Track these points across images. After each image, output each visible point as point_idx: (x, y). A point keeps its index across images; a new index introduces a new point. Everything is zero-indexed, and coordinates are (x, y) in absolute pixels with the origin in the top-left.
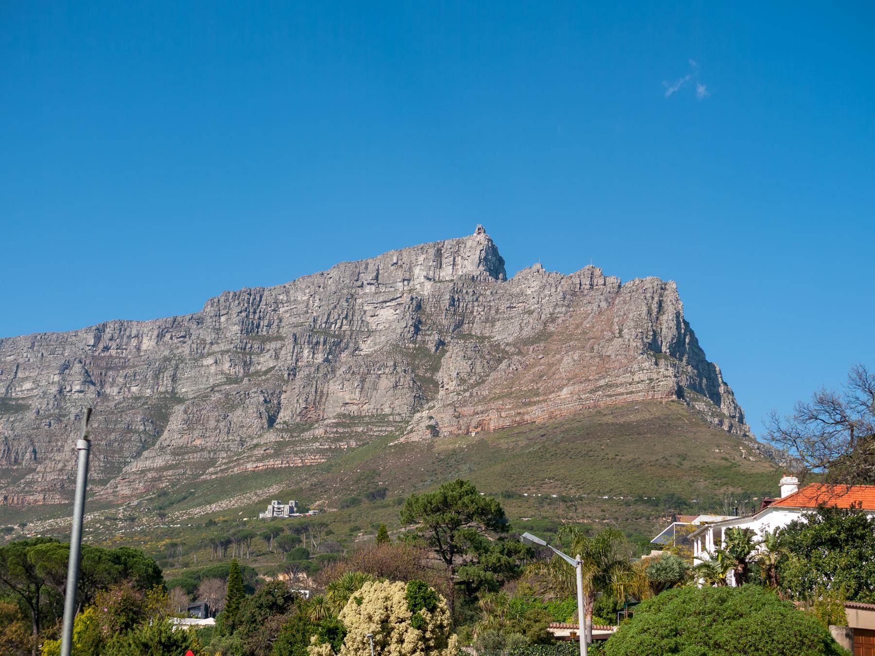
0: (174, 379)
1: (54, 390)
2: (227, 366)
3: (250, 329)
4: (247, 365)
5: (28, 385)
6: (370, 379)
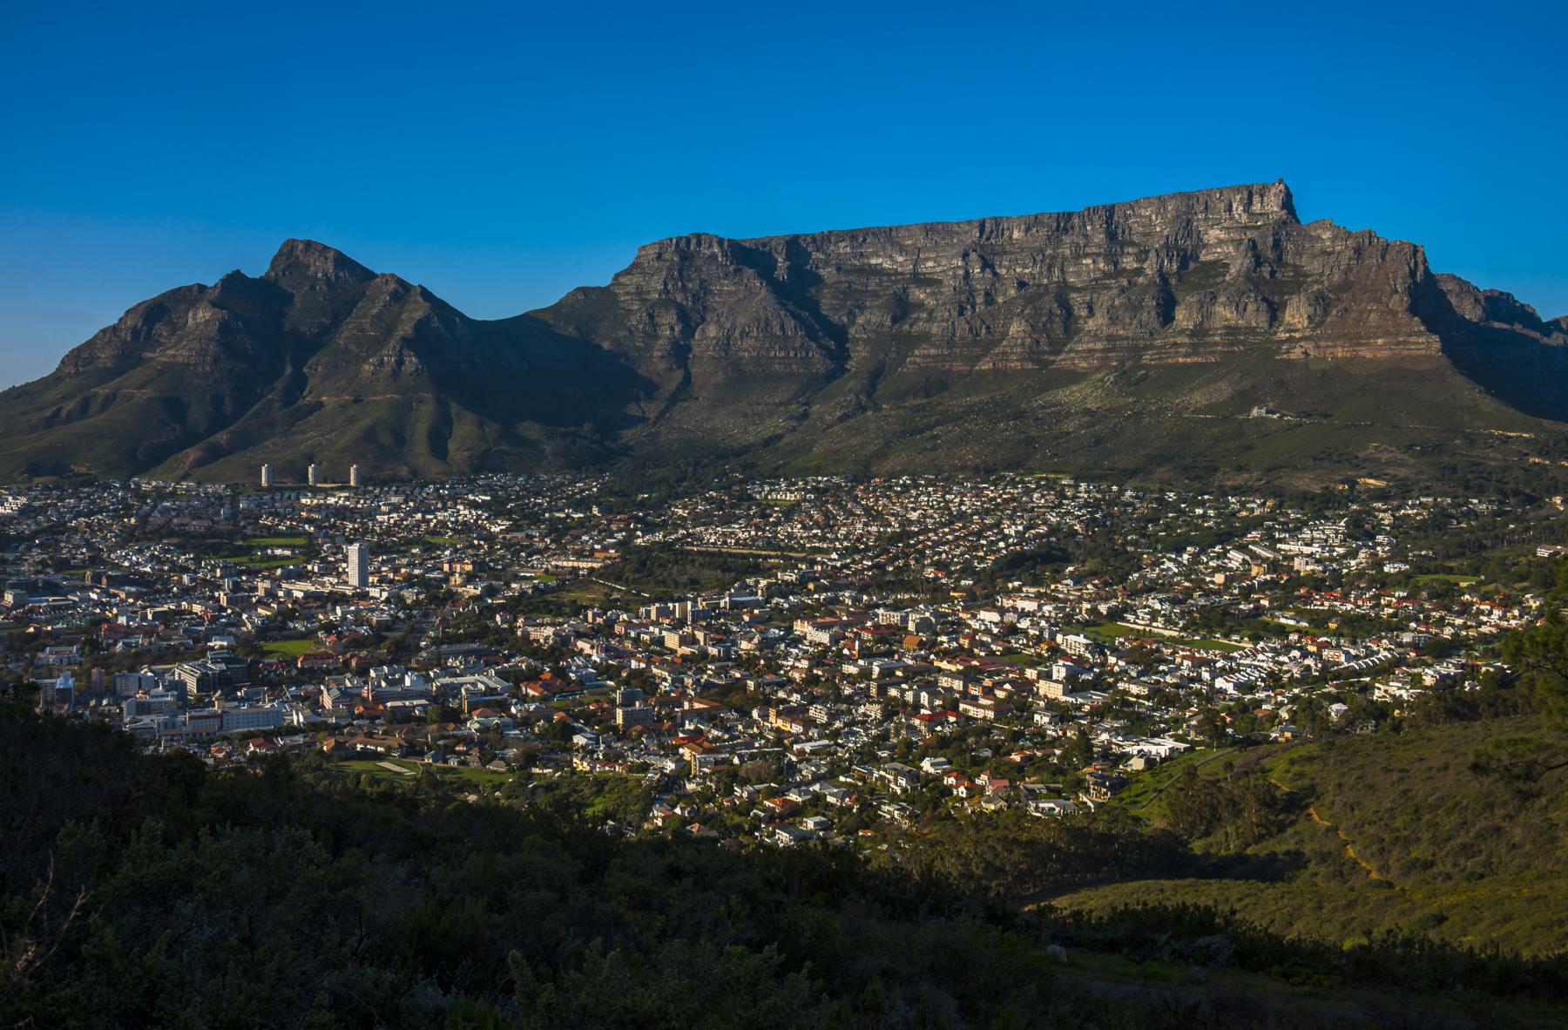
0: (1063, 271)
1: (961, 272)
2: (1101, 265)
3: (1111, 236)
4: (1116, 264)
5: (930, 264)
6: (1241, 306)
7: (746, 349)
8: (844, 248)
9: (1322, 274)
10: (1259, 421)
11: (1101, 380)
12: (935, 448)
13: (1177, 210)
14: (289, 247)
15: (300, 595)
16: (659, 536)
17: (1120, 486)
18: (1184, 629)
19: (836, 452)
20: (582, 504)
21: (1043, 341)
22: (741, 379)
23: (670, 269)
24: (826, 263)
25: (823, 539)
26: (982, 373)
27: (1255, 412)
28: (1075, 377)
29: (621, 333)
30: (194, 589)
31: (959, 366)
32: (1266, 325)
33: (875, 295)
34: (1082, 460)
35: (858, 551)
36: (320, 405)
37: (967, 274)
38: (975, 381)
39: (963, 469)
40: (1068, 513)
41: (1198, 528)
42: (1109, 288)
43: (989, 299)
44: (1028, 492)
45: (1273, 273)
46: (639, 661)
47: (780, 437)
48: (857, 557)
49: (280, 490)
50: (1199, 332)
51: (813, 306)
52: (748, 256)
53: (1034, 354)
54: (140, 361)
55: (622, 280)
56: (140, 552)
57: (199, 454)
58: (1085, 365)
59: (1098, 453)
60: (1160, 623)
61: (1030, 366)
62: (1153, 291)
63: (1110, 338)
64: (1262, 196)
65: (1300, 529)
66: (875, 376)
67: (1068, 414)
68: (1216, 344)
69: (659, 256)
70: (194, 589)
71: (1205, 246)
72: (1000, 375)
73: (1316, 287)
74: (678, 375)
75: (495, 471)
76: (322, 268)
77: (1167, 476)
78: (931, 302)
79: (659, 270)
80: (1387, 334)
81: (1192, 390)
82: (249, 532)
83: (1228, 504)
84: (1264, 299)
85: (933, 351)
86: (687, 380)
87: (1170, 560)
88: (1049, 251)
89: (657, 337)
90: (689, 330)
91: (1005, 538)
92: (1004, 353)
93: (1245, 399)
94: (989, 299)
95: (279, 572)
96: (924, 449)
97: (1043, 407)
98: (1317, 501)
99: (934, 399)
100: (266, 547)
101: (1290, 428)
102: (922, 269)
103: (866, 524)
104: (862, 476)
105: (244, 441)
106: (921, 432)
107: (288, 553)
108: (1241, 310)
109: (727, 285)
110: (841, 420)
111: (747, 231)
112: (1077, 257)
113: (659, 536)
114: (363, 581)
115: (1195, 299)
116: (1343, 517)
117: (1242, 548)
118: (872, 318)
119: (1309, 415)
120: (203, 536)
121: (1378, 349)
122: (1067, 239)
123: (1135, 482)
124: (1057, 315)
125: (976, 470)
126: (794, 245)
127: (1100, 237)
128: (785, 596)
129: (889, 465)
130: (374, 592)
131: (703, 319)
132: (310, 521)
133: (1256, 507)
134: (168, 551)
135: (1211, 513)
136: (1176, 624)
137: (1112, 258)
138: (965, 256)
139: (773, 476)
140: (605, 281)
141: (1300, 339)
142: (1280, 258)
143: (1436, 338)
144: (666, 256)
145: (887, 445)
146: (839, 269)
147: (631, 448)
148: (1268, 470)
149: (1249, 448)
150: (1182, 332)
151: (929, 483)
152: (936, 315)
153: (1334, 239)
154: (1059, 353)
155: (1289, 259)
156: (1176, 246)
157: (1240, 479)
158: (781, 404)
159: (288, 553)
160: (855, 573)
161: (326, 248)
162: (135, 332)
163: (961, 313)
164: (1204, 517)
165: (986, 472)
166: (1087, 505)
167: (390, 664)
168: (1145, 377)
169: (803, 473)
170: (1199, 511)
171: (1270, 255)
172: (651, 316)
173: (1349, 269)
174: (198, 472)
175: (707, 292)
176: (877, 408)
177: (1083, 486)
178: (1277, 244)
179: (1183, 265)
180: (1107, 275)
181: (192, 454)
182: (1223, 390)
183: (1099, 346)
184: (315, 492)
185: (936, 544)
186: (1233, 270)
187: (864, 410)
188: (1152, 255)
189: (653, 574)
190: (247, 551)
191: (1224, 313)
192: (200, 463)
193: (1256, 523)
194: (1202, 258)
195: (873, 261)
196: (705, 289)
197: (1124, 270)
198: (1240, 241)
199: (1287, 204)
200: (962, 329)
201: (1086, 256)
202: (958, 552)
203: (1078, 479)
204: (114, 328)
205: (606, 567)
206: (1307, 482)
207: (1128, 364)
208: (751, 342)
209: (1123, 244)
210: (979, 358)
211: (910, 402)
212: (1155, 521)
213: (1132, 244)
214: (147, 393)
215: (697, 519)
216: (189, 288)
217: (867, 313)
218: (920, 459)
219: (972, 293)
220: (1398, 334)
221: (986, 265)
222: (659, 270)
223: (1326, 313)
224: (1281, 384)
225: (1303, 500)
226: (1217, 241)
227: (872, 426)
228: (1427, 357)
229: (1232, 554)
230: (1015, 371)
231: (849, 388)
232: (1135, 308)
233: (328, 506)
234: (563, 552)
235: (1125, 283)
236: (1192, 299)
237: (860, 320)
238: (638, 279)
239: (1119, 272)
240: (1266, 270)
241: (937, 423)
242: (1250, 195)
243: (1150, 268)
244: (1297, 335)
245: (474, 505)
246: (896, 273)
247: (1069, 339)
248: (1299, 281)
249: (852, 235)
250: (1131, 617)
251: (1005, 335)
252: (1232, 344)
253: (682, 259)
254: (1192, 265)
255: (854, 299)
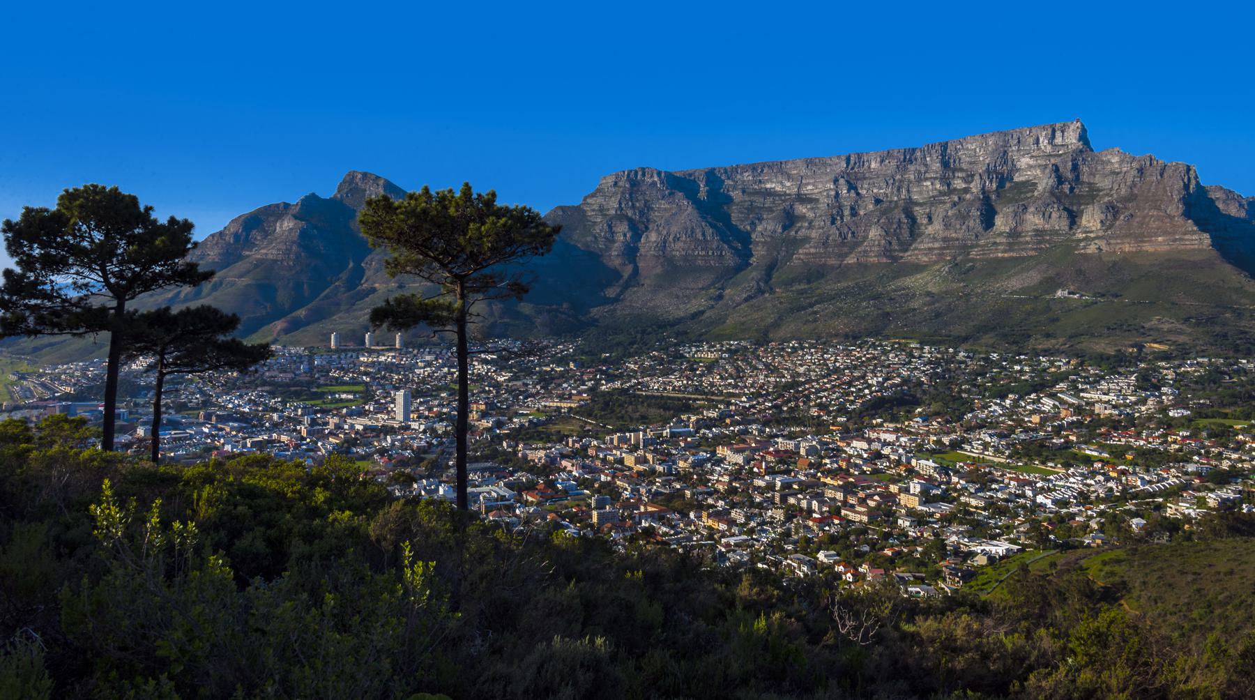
1: (833, 193)
2: (938, 186)
3: (945, 164)
4: (949, 185)
5: (810, 187)
6: (1047, 215)
7: (678, 249)
8: (748, 177)
9: (1111, 189)
10: (1063, 301)
11: (939, 270)
12: (815, 320)
13: (996, 144)
14: (350, 180)
15: (361, 428)
16: (618, 384)
17: (955, 348)
18: (1010, 457)
19: (743, 324)
20: (562, 361)
21: (894, 242)
22: (674, 271)
23: (623, 193)
24: (735, 188)
25: (735, 386)
26: (849, 267)
27: (1059, 293)
28: (918, 268)
29: (589, 239)
30: (282, 424)
31: (832, 261)
32: (1067, 228)
33: (770, 210)
34: (925, 330)
35: (762, 396)
36: (374, 290)
37: (837, 195)
38: (843, 272)
39: (837, 335)
40: (916, 368)
41: (1016, 380)
42: (944, 203)
43: (854, 213)
44: (885, 353)
45: (1072, 189)
46: (607, 475)
47: (702, 312)
48: (761, 400)
49: (345, 351)
50: (1014, 234)
51: (727, 218)
52: (679, 184)
53: (887, 252)
54: (240, 258)
55: (589, 201)
56: (241, 397)
57: (285, 325)
58: (926, 259)
59: (938, 326)
60: (990, 452)
61: (884, 260)
62: (978, 204)
63: (945, 240)
64: (1063, 132)
65: (1098, 382)
66: (771, 268)
67: (914, 295)
68: (1027, 243)
69: (616, 184)
70: (282, 424)
71: (1018, 170)
72: (862, 267)
73: (1106, 199)
74: (629, 269)
75: (500, 338)
76: (375, 192)
77: (991, 341)
78: (810, 215)
79: (615, 194)
80: (1165, 233)
81: (1009, 278)
82: (322, 381)
83: (1040, 363)
84: (1065, 209)
85: (812, 250)
86: (636, 271)
87: (996, 404)
88: (898, 177)
89: (614, 241)
90: (637, 236)
91: (869, 386)
92: (865, 251)
93: (1051, 284)
94: (854, 213)
95: (345, 411)
96: (808, 321)
97: (895, 291)
98: (1112, 360)
99: (814, 285)
100: (335, 393)
101: (1087, 305)
102: (804, 191)
103: (766, 376)
104: (762, 340)
105: (319, 315)
106: (804, 308)
107: (351, 397)
108: (1047, 217)
109: (664, 204)
110: (746, 300)
111: (679, 167)
112: (920, 180)
113: (618, 384)
114: (406, 418)
115: (1011, 209)
116: (1133, 373)
117: (1053, 396)
118: (768, 227)
119: (1103, 295)
120: (288, 385)
121: (1159, 245)
122: (912, 168)
123: (964, 346)
124: (905, 223)
125: (846, 336)
126: (711, 175)
127: (937, 166)
128: (709, 428)
129: (783, 332)
130: (414, 425)
131: (647, 228)
132: (366, 374)
133: (1062, 364)
134: (262, 396)
135: (1027, 369)
136: (1003, 453)
137: (946, 181)
138: (836, 181)
139: (698, 340)
140: (577, 202)
141: (1094, 239)
142: (1077, 178)
143: (1207, 236)
144: (621, 184)
145: (780, 318)
146: (744, 192)
147: (597, 320)
148: (1071, 337)
149: (1057, 320)
150: (1001, 234)
151: (812, 346)
152: (815, 226)
153: (1121, 162)
154: (907, 250)
155: (1085, 178)
156: (995, 171)
157: (1048, 344)
158: (703, 289)
159: (351, 397)
160: (759, 412)
161: (378, 178)
162: (236, 236)
163: (833, 223)
164: (1021, 371)
165: (854, 338)
166: (930, 362)
167: (428, 478)
168: (973, 268)
169: (720, 338)
170: (1017, 368)
171: (1070, 176)
172: (610, 227)
173: (1134, 184)
174: (284, 338)
175: (650, 209)
176: (772, 291)
177: (927, 348)
178: (1075, 168)
179: (1001, 185)
180: (941, 193)
181: (279, 325)
182: (1033, 277)
183: (937, 245)
184: (370, 352)
185: (818, 391)
186: (1040, 188)
187: (763, 293)
188: (977, 178)
189: (615, 411)
190: (321, 396)
191: (1033, 220)
192: (287, 331)
193: (1063, 377)
194: (1016, 179)
195: (768, 186)
196: (648, 206)
197: (955, 189)
198: (1046, 166)
199: (1083, 137)
200: (834, 231)
201: (926, 179)
202: (834, 396)
203: (923, 343)
204: (221, 233)
205: (581, 406)
206: (1104, 346)
207: (959, 258)
208: (680, 245)
209: (954, 171)
210: (846, 255)
211: (797, 287)
212: (983, 374)
213: (961, 170)
214: (246, 281)
215: (645, 372)
216: (277, 206)
217: (764, 223)
218: (806, 328)
219: (840, 208)
220: (1174, 233)
221: (852, 187)
222: (615, 194)
223: (1115, 217)
224: (1080, 272)
225: (1100, 359)
226: (1028, 167)
227: (769, 305)
228: (1200, 250)
229: (1045, 400)
230: (873, 265)
231: (752, 277)
232: (963, 217)
233: (380, 363)
234: (549, 395)
235: (956, 199)
236: (1009, 209)
237: (759, 228)
238: (600, 200)
239: (951, 191)
240: (1066, 188)
241: (817, 302)
242: (1054, 131)
243: (975, 187)
244: (1092, 235)
245: (485, 362)
246: (785, 194)
247: (914, 240)
248: (1093, 195)
249: (754, 168)
250: (968, 447)
251: (866, 238)
252: (1040, 243)
253: (631, 185)
254: (1008, 185)
255: (755, 212)
